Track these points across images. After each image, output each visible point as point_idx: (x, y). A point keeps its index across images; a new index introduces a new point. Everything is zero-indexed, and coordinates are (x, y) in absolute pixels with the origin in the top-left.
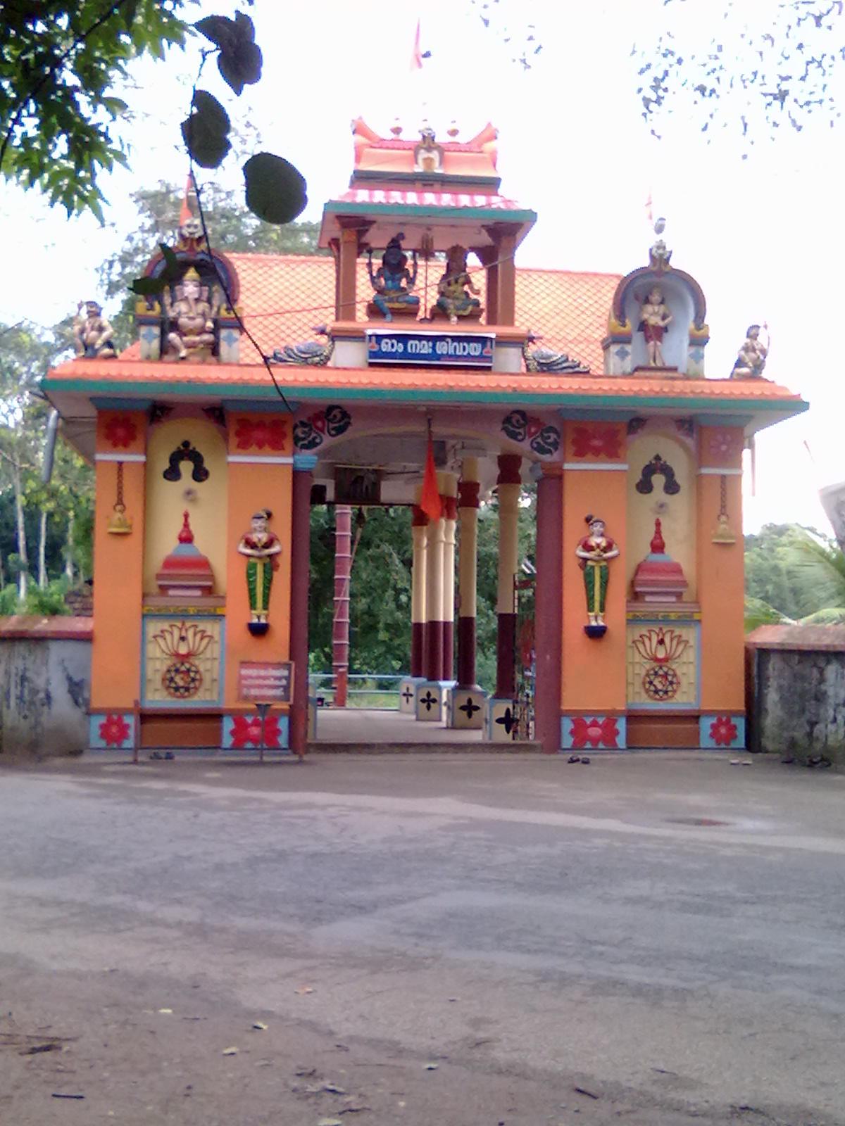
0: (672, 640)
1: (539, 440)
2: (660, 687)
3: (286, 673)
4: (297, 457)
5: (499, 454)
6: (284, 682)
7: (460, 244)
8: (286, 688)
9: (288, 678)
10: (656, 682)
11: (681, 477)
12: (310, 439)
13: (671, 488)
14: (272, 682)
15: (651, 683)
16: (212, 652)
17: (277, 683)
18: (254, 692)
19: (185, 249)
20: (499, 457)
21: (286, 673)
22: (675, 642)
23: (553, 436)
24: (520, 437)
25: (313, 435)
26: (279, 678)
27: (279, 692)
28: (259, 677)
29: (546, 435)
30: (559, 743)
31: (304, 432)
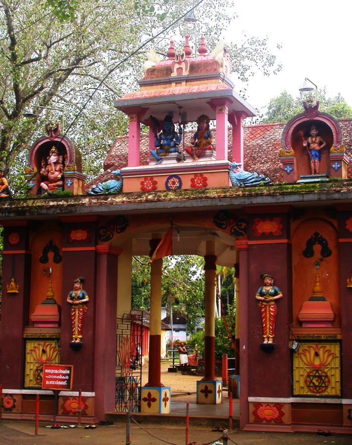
0: (324, 353)
1: (236, 227)
2: (317, 384)
3: (68, 372)
4: (98, 246)
5: (151, 239)
6: (67, 377)
7: (205, 114)
8: (68, 381)
9: (69, 375)
10: (314, 381)
11: (331, 246)
12: (107, 235)
13: (326, 252)
14: (61, 377)
15: (311, 382)
16: (176, 362)
17: (64, 377)
18: (52, 382)
19: (48, 137)
20: (150, 241)
21: (68, 372)
22: (326, 355)
23: (244, 225)
24: (224, 226)
25: (109, 233)
26: (65, 375)
27: (64, 383)
28: (54, 374)
29: (239, 224)
30: (249, 421)
31: (104, 232)
